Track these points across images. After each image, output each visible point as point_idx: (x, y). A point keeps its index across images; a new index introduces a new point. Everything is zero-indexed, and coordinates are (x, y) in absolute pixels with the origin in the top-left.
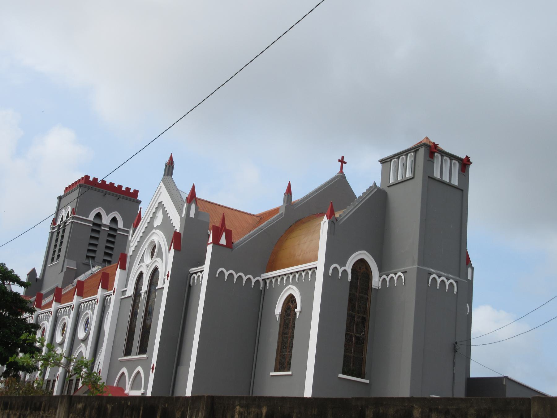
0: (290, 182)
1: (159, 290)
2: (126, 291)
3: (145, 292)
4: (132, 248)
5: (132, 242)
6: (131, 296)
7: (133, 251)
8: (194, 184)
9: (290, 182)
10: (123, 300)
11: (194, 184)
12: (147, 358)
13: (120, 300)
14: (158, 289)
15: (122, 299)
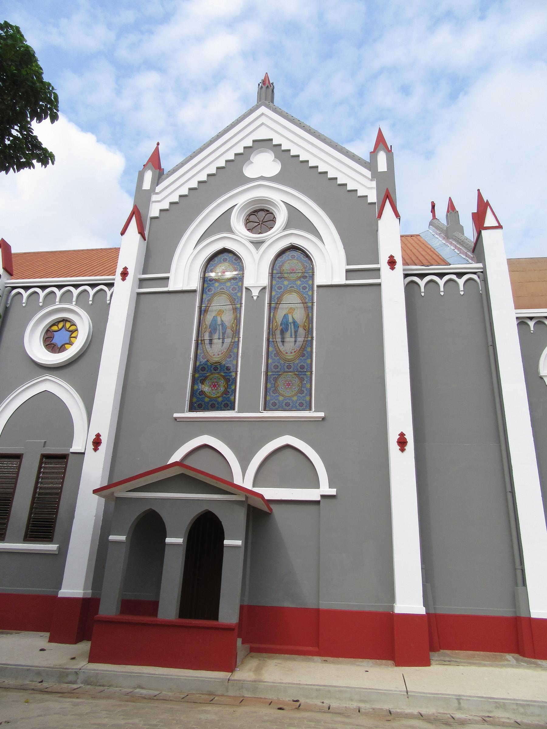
0: (450, 199)
1: (321, 289)
2: (167, 278)
3: (264, 288)
4: (154, 204)
5: (157, 193)
6: (194, 291)
7: (161, 211)
8: (380, 128)
9: (450, 199)
10: (143, 297)
11: (380, 128)
12: (321, 420)
13: (135, 296)
14: (318, 286)
15: (139, 294)
